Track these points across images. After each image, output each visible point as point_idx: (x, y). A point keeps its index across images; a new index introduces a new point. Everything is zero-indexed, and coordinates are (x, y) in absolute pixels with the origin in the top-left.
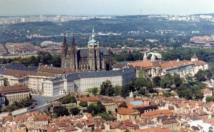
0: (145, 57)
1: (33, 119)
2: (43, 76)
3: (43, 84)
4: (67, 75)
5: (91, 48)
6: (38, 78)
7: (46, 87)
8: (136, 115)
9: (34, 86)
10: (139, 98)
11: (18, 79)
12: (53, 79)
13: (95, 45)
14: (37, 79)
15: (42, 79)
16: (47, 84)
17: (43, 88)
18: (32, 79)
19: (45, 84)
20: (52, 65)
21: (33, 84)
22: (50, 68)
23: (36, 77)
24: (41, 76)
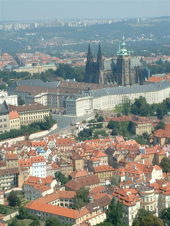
1: (54, 144)
5: (120, 58)
7: (68, 106)
11: (35, 97)
15: (63, 97)
18: (51, 96)
19: (67, 102)
20: (74, 79)
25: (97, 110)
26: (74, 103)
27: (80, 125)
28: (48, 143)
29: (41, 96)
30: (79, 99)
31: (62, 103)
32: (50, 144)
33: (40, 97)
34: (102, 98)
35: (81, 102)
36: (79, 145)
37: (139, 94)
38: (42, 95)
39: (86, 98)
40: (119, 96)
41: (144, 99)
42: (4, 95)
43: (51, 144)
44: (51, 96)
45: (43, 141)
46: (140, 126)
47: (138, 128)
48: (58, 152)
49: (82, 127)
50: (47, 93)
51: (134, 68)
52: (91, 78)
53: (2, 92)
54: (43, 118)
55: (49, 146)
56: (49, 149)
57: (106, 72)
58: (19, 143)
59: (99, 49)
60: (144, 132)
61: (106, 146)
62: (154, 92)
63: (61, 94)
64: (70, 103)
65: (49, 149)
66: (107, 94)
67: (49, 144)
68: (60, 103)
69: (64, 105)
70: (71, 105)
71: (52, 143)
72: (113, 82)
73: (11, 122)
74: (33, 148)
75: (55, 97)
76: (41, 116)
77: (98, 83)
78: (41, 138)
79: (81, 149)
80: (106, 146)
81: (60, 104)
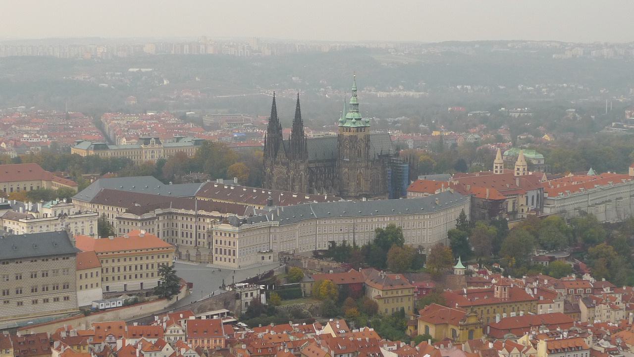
0: (498, 160)
1: (181, 332)
2: (211, 212)
3: (210, 233)
4: (280, 209)
5: (347, 134)
6: (198, 216)
7: (219, 242)
8: (470, 329)
9: (185, 239)
10: (480, 279)
11: (139, 218)
12: (240, 220)
13: (359, 126)
14: (194, 220)
15: (208, 220)
16: (221, 234)
17: (210, 244)
18: (180, 218)
19: (217, 234)
20: (235, 180)
21: (183, 233)
22: (232, 188)
23: (192, 212)
24: (206, 211)
25: (288, 254)
26: (232, 236)
27: (246, 289)
28: (165, 331)
29: (155, 216)
30: (245, 226)
31: (204, 234)
32: (171, 332)
33: (154, 218)
34: (299, 225)
35: (248, 234)
36: (241, 336)
37: (387, 219)
38: (157, 215)
39: (261, 224)
40: (339, 222)
41: (399, 229)
42: (65, 211)
43: (174, 333)
44: (180, 218)
45: (155, 324)
46: (387, 296)
47: (383, 300)
48: (188, 352)
49: (249, 295)
50: (166, 211)
51: (377, 158)
52: (275, 179)
53: (62, 205)
54: (156, 269)
55: (169, 339)
56: (168, 344)
57: (312, 165)
58: (98, 328)
59: (298, 110)
60: (395, 310)
61: (305, 341)
62: (421, 217)
63: (203, 213)
64: (223, 235)
65: (168, 344)
66: (312, 218)
67: (168, 333)
68: (199, 234)
69: (208, 240)
70: (225, 242)
71: (176, 331)
72: (326, 188)
73: (81, 277)
74: (130, 342)
75: (189, 219)
76: (153, 265)
77: (293, 189)
78: (148, 320)
79: (244, 346)
80: (305, 341)
81: (199, 238)
